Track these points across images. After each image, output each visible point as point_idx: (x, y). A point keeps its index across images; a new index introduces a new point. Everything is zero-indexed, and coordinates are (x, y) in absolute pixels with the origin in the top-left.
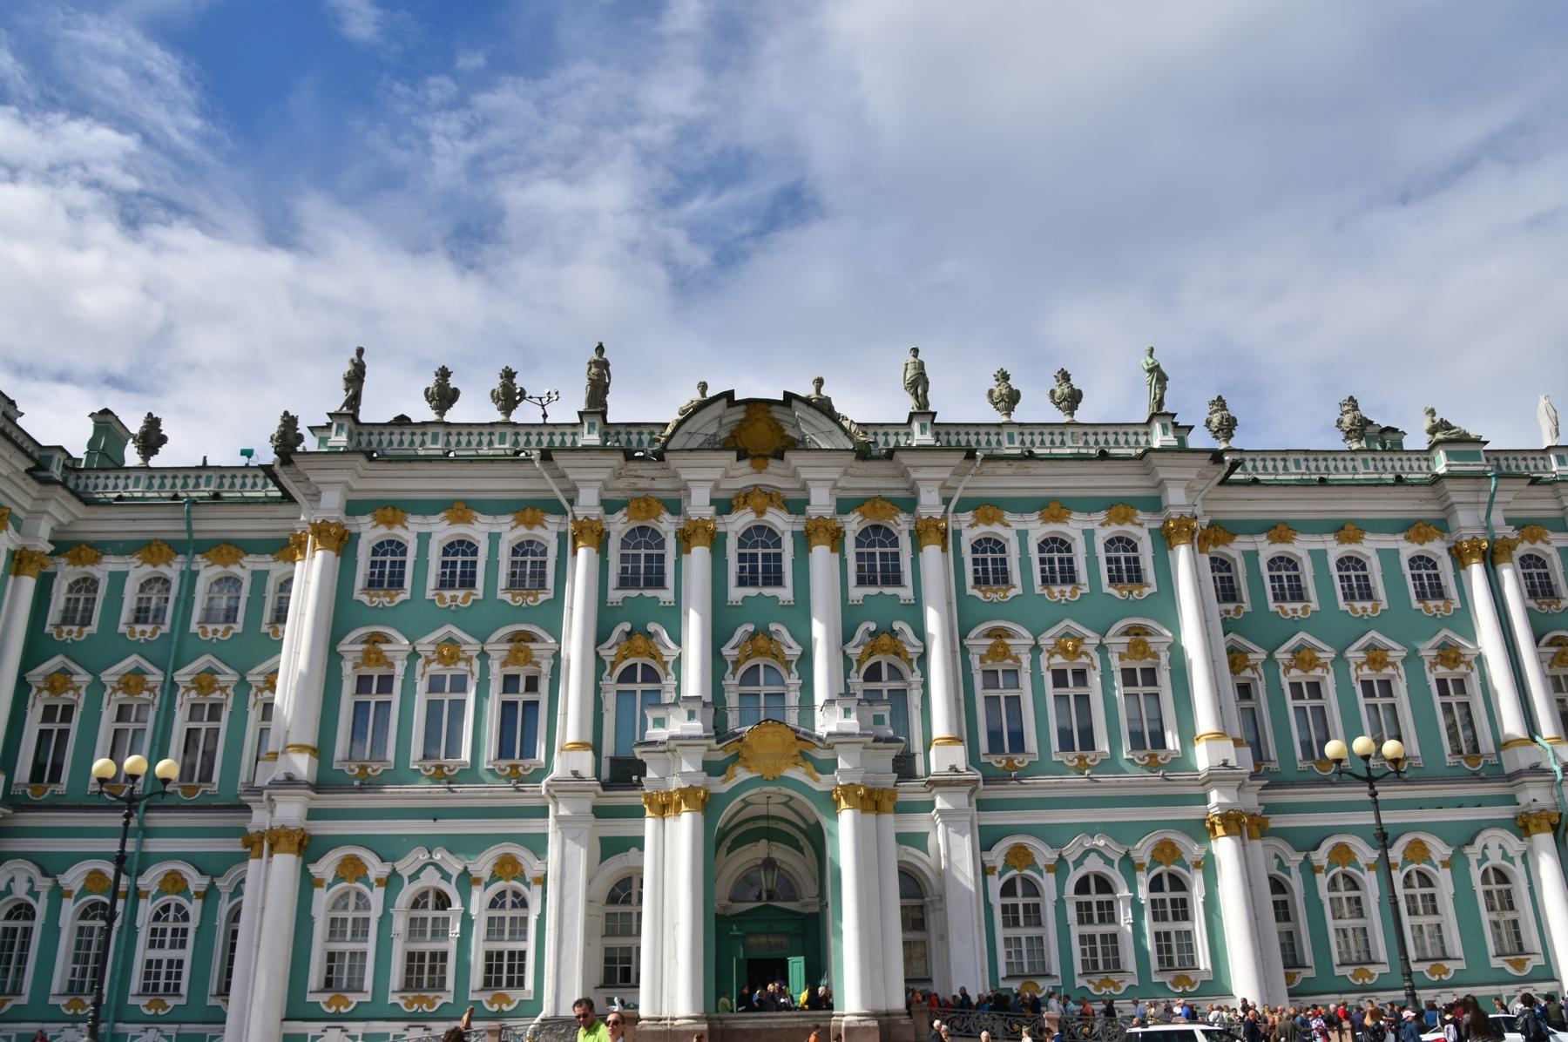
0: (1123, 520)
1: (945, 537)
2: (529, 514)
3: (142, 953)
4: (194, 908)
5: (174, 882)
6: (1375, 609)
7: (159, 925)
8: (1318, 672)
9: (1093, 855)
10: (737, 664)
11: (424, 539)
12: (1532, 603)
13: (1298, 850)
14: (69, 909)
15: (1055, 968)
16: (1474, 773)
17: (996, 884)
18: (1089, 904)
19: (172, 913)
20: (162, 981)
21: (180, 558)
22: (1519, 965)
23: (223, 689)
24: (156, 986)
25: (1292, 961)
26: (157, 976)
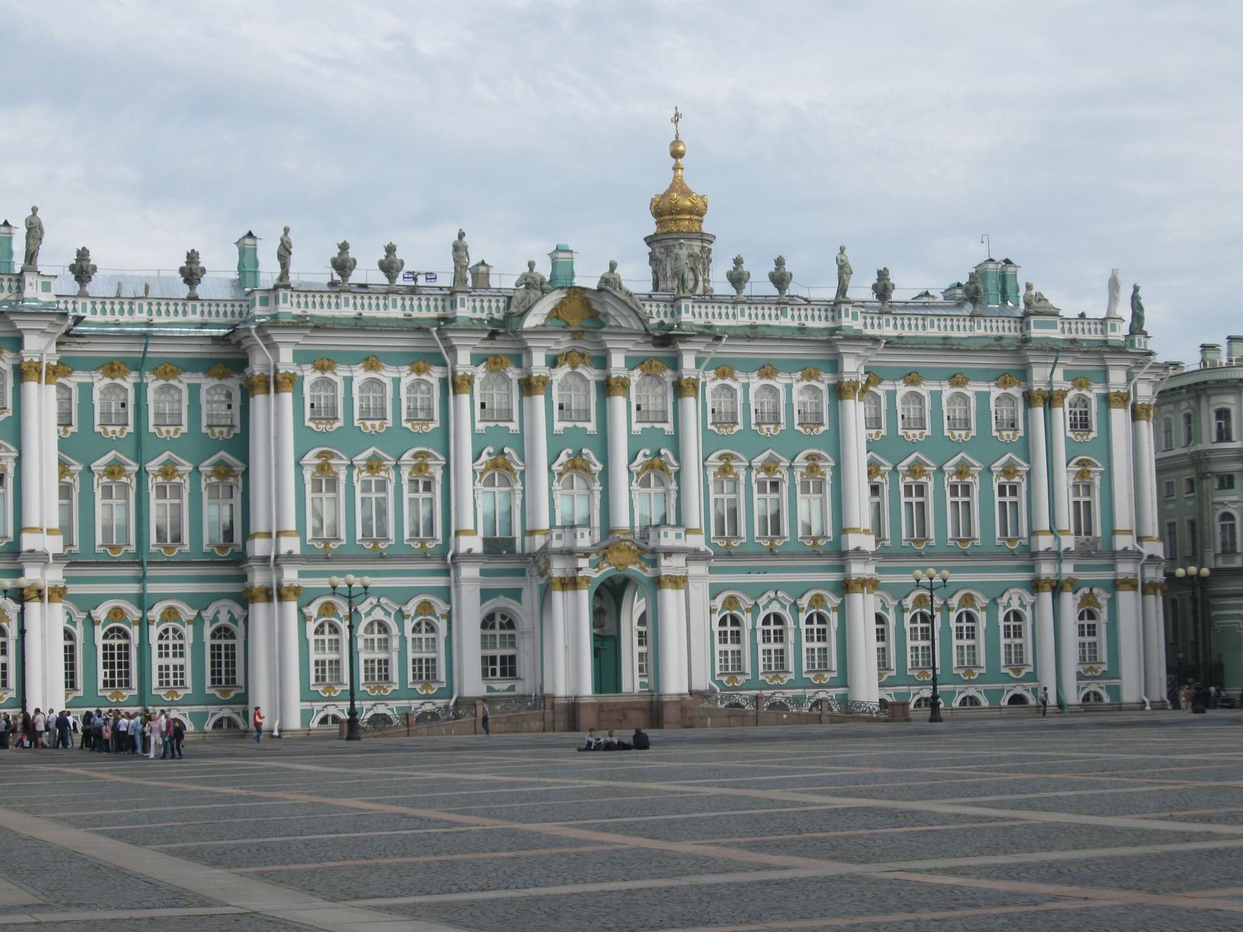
0: (810, 377)
1: (695, 388)
2: (422, 365)
3: (156, 662)
4: (188, 631)
5: (170, 614)
6: (967, 436)
7: (164, 642)
8: (923, 479)
9: (775, 603)
10: (560, 474)
11: (349, 381)
12: (1070, 434)
13: (895, 599)
14: (99, 632)
15: (748, 669)
16: (1012, 551)
17: (716, 618)
18: (769, 632)
19: (171, 634)
20: (172, 679)
21: (134, 374)
22: (1017, 671)
23: (181, 476)
24: (168, 683)
25: (883, 665)
26: (167, 675)
